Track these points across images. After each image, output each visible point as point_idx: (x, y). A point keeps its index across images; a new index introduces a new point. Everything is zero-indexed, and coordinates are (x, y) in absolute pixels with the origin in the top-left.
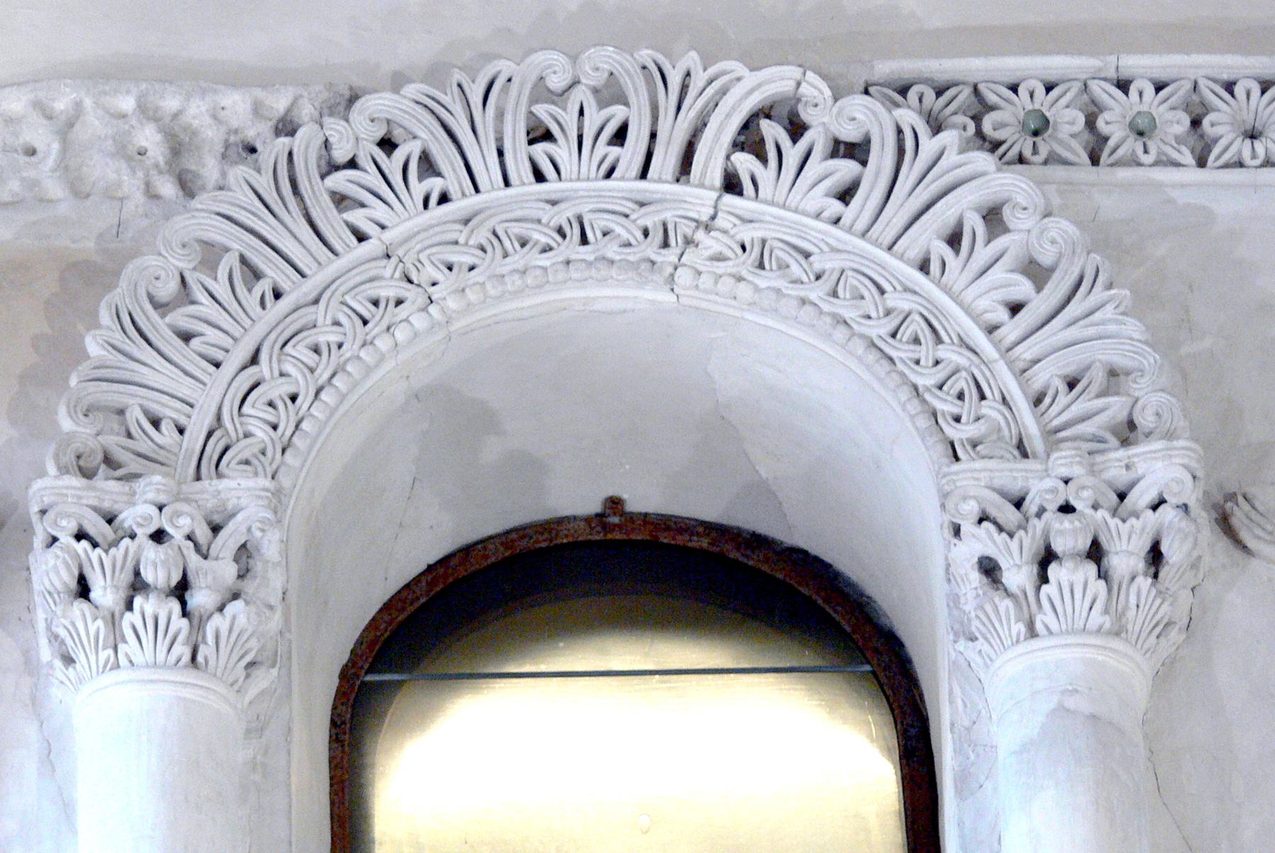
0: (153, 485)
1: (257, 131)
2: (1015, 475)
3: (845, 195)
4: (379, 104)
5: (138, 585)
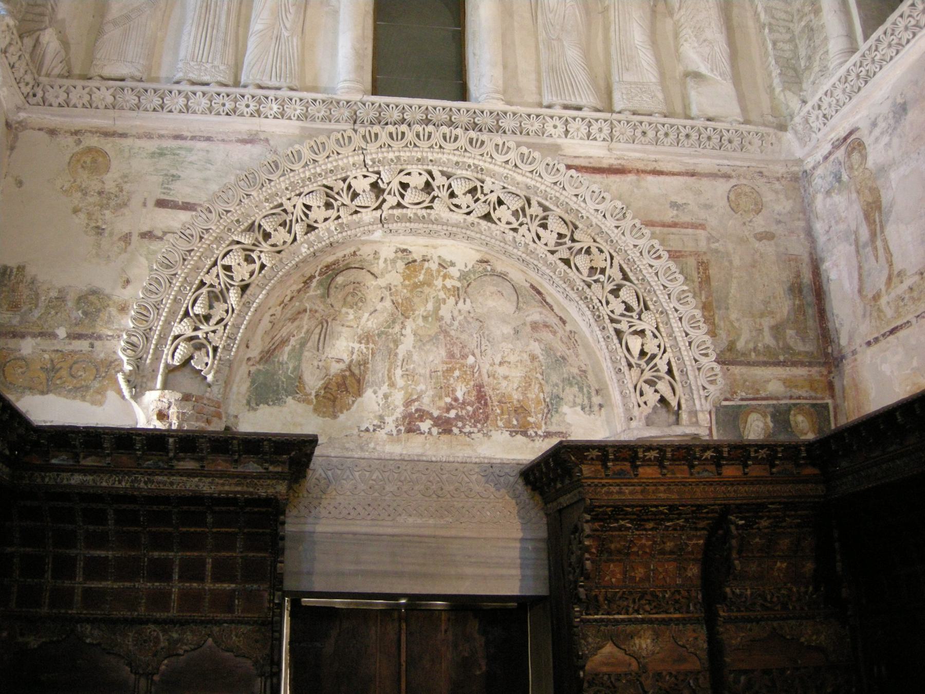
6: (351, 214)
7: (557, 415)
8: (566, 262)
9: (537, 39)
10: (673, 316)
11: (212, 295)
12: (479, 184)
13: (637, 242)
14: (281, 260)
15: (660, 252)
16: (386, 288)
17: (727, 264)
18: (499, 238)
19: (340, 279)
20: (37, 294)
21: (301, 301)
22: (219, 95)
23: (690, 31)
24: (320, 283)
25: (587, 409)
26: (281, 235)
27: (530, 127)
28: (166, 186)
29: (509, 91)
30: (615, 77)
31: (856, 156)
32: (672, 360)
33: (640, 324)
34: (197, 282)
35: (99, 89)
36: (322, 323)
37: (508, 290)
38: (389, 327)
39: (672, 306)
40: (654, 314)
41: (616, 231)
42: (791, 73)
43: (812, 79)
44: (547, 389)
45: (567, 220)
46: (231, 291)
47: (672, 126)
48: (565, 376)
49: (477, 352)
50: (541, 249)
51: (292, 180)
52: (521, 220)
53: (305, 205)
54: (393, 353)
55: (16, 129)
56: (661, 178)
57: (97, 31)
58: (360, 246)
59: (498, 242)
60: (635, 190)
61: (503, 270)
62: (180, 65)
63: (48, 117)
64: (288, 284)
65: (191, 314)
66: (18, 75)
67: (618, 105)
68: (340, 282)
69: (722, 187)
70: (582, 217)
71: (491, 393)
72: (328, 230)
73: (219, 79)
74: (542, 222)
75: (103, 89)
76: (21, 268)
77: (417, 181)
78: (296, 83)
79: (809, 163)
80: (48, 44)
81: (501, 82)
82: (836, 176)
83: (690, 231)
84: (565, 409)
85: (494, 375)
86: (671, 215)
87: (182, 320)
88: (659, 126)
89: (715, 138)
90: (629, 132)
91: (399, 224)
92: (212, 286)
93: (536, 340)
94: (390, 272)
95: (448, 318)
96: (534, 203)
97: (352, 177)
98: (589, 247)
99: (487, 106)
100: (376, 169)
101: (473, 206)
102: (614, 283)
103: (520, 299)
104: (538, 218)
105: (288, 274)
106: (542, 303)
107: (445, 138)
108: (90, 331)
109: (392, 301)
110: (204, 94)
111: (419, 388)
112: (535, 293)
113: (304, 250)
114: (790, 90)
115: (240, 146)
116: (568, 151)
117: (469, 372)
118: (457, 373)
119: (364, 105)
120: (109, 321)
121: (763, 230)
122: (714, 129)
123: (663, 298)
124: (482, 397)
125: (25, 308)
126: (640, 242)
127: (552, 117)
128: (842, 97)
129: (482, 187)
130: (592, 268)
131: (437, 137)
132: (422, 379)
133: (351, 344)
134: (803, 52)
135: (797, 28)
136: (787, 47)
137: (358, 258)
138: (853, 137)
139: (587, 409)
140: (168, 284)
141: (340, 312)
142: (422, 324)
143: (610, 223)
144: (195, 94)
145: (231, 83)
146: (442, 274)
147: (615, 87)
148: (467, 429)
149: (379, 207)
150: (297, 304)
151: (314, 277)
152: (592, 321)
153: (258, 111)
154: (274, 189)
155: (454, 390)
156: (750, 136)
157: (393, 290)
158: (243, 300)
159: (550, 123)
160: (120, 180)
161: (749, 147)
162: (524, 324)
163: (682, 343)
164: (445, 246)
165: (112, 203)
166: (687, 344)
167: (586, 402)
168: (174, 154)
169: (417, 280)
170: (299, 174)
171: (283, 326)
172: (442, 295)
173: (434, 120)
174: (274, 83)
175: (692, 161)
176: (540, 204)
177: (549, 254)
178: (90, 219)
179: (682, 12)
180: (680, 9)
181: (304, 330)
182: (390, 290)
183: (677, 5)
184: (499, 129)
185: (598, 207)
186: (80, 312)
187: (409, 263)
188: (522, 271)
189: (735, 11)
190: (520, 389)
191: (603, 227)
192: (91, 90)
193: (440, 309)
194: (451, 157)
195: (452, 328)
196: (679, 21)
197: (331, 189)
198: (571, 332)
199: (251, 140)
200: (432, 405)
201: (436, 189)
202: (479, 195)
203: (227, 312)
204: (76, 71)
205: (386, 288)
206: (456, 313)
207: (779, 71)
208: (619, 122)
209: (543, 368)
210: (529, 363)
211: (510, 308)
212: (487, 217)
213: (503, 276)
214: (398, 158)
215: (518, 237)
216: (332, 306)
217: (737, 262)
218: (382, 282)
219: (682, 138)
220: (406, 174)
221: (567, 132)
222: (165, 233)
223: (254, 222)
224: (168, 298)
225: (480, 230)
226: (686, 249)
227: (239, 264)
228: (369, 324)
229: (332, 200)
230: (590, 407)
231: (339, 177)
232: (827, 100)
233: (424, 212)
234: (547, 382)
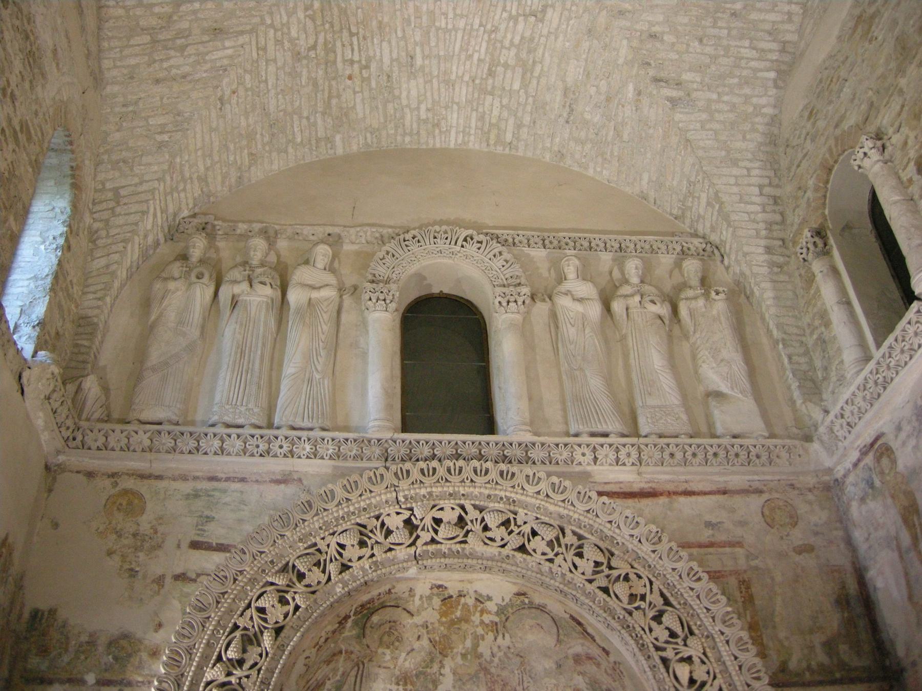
0: (381, 285)
1: (394, 235)
2: (504, 290)
3: (479, 249)
4: (413, 232)
5: (378, 299)
6: (386, 552)
8: (605, 590)
9: (559, 370)
10: (719, 639)
11: (245, 638)
12: (512, 516)
14: (315, 601)
15: (701, 574)
16: (422, 626)
17: (769, 580)
18: (535, 569)
19: (375, 619)
20: (67, 638)
21: (336, 642)
22: (253, 436)
23: (707, 353)
24: (356, 623)
26: (314, 576)
27: (558, 456)
28: (200, 527)
29: (535, 423)
30: (639, 403)
31: (885, 461)
34: (230, 625)
35: (136, 433)
36: (358, 665)
37: (548, 623)
38: (427, 667)
39: (717, 629)
41: (653, 555)
42: (809, 384)
43: (830, 389)
45: (603, 547)
46: (265, 634)
47: (699, 446)
50: (579, 579)
51: (326, 519)
52: (556, 549)
53: (338, 544)
55: (55, 471)
56: (693, 499)
57: (136, 377)
58: (394, 584)
59: (534, 574)
60: (669, 513)
62: (216, 409)
63: (86, 460)
64: (323, 625)
65: (224, 659)
66: (59, 420)
67: (644, 430)
68: (375, 621)
69: (756, 502)
70: (618, 543)
72: (362, 569)
73: (253, 421)
75: (141, 432)
76: (52, 612)
77: (449, 516)
78: (328, 424)
79: (840, 472)
80: (89, 389)
81: (527, 415)
82: (868, 482)
83: (728, 550)
86: (707, 534)
87: (214, 665)
88: (687, 447)
89: (743, 454)
90: (657, 455)
91: (434, 560)
92: (245, 629)
93: (580, 673)
95: (487, 654)
96: (568, 532)
97: (385, 514)
98: (627, 574)
99: (515, 438)
100: (409, 506)
101: (507, 538)
102: (656, 609)
103: (561, 631)
104: (574, 548)
105: (322, 615)
107: (475, 471)
108: (120, 677)
109: (430, 639)
110: (239, 436)
113: (338, 590)
114: (811, 401)
115: (275, 487)
116: (598, 478)
119: (395, 442)
120: (140, 666)
121: (801, 543)
122: (741, 446)
123: (707, 622)
125: (54, 653)
126: (678, 565)
127: (580, 446)
128: (862, 404)
129: (515, 519)
130: (631, 595)
131: (468, 472)
133: (389, 686)
134: (818, 363)
135: (810, 341)
136: (803, 360)
137: (393, 596)
138: (879, 443)
140: (201, 628)
141: (376, 652)
142: (461, 662)
143: (646, 548)
144: (230, 436)
145: (264, 425)
146: (479, 609)
147: (639, 411)
149: (413, 544)
150: (332, 645)
151: (350, 617)
152: (636, 650)
153: (291, 451)
154: (307, 529)
156: (777, 450)
157: (430, 627)
158: (278, 643)
159: (579, 451)
160: (154, 522)
161: (778, 461)
162: (566, 657)
163: (732, 668)
164: (482, 580)
165: (147, 545)
166: (737, 668)
168: (209, 496)
170: (332, 514)
171: (319, 668)
172: (480, 631)
173: (464, 454)
174: (307, 425)
175: (722, 479)
176: (574, 533)
177: (587, 584)
178: (123, 561)
179: (697, 335)
180: (694, 332)
181: (340, 673)
182: (427, 627)
183: (692, 329)
184: (528, 460)
185: (632, 532)
186: (110, 657)
187: (445, 599)
189: (748, 329)
191: (639, 552)
192: (129, 434)
193: (478, 646)
194: (482, 490)
196: (695, 343)
197: (364, 527)
198: (615, 663)
199: (284, 480)
201: (469, 523)
202: (512, 527)
203: (261, 655)
204: (115, 415)
205: (422, 626)
206: (495, 650)
207: (797, 384)
208: (647, 446)
211: (550, 641)
212: (522, 549)
213: (541, 608)
214: (430, 494)
215: (555, 568)
216: (368, 647)
217: (779, 578)
218: (418, 620)
219: (710, 457)
221: (595, 459)
222: (198, 575)
223: (288, 563)
224: (201, 643)
227: (273, 606)
228: (407, 664)
229: (366, 539)
231: (372, 514)
232: (848, 408)
233: (458, 547)
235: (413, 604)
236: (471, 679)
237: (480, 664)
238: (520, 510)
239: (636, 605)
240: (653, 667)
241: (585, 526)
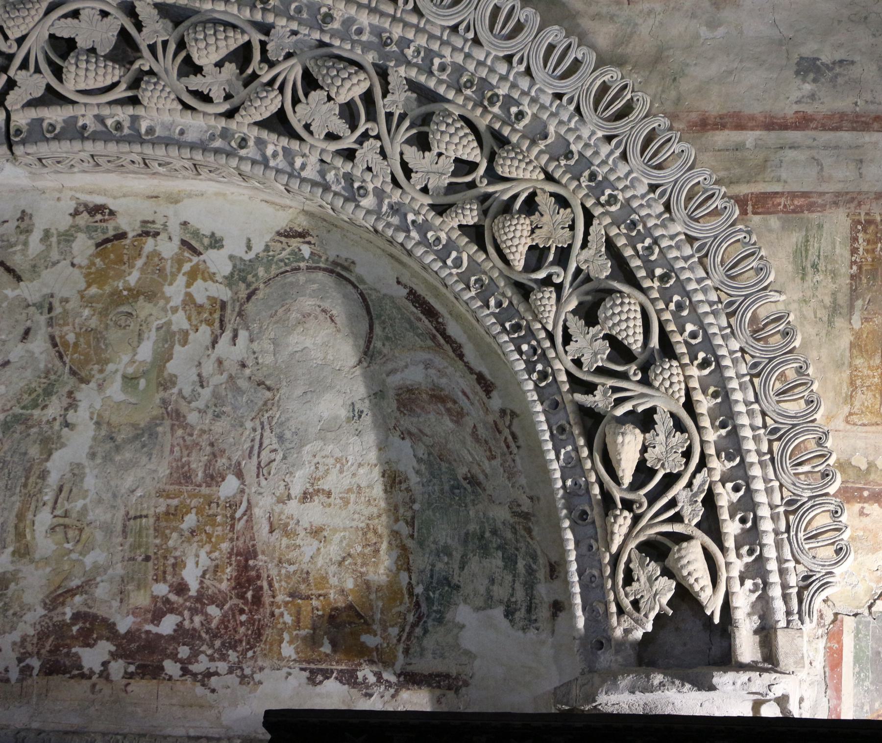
7: (441, 630)
8: (476, 234)
12: (256, 37)
13: (659, 177)
25: (520, 615)
32: (719, 489)
33: (642, 395)
39: (735, 345)
40: (683, 366)
41: (605, 149)
44: (420, 561)
45: (483, 123)
48: (472, 527)
49: (250, 467)
54: (36, 471)
61: (344, 254)
70: (520, 115)
71: (274, 572)
74: (414, 131)
84: (463, 613)
85: (286, 525)
94: (54, 264)
95: (186, 383)
98: (533, 195)
101: (241, 93)
102: (587, 287)
103: (378, 330)
104: (407, 123)
106: (433, 338)
109: (52, 338)
111: (89, 560)
112: (418, 312)
117: (219, 519)
118: (190, 520)
124: (250, 581)
129: (263, 44)
132: (99, 536)
139: (520, 615)
146: (187, 267)
148: (201, 665)
155: (178, 565)
157: (58, 310)
167: (520, 594)
169: (121, 285)
172: (180, 321)
176: (413, 86)
182: (50, 310)
187: (107, 241)
188: (392, 256)
190: (349, 561)
193: (170, 358)
195: (193, 405)
200: (116, 604)
201: (146, 53)
202: (255, 64)
205: (39, 306)
206: (208, 368)
209: (416, 507)
210: (378, 491)
218: (31, 290)
220: (65, 16)
225: (264, 155)
226: (824, 188)
230: (529, 610)
234: (421, 544)
235: (24, 252)
236: (137, 437)
237: (165, 402)
238: (282, 22)
239: (541, 275)
240: (560, 434)
241: (443, 68)
